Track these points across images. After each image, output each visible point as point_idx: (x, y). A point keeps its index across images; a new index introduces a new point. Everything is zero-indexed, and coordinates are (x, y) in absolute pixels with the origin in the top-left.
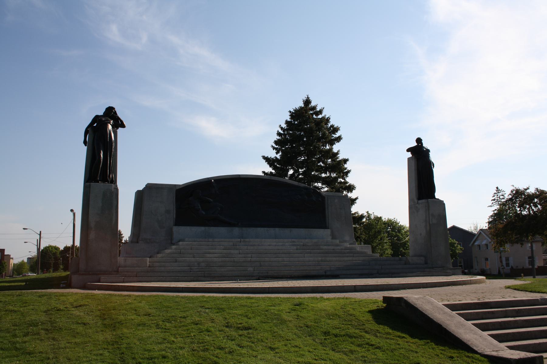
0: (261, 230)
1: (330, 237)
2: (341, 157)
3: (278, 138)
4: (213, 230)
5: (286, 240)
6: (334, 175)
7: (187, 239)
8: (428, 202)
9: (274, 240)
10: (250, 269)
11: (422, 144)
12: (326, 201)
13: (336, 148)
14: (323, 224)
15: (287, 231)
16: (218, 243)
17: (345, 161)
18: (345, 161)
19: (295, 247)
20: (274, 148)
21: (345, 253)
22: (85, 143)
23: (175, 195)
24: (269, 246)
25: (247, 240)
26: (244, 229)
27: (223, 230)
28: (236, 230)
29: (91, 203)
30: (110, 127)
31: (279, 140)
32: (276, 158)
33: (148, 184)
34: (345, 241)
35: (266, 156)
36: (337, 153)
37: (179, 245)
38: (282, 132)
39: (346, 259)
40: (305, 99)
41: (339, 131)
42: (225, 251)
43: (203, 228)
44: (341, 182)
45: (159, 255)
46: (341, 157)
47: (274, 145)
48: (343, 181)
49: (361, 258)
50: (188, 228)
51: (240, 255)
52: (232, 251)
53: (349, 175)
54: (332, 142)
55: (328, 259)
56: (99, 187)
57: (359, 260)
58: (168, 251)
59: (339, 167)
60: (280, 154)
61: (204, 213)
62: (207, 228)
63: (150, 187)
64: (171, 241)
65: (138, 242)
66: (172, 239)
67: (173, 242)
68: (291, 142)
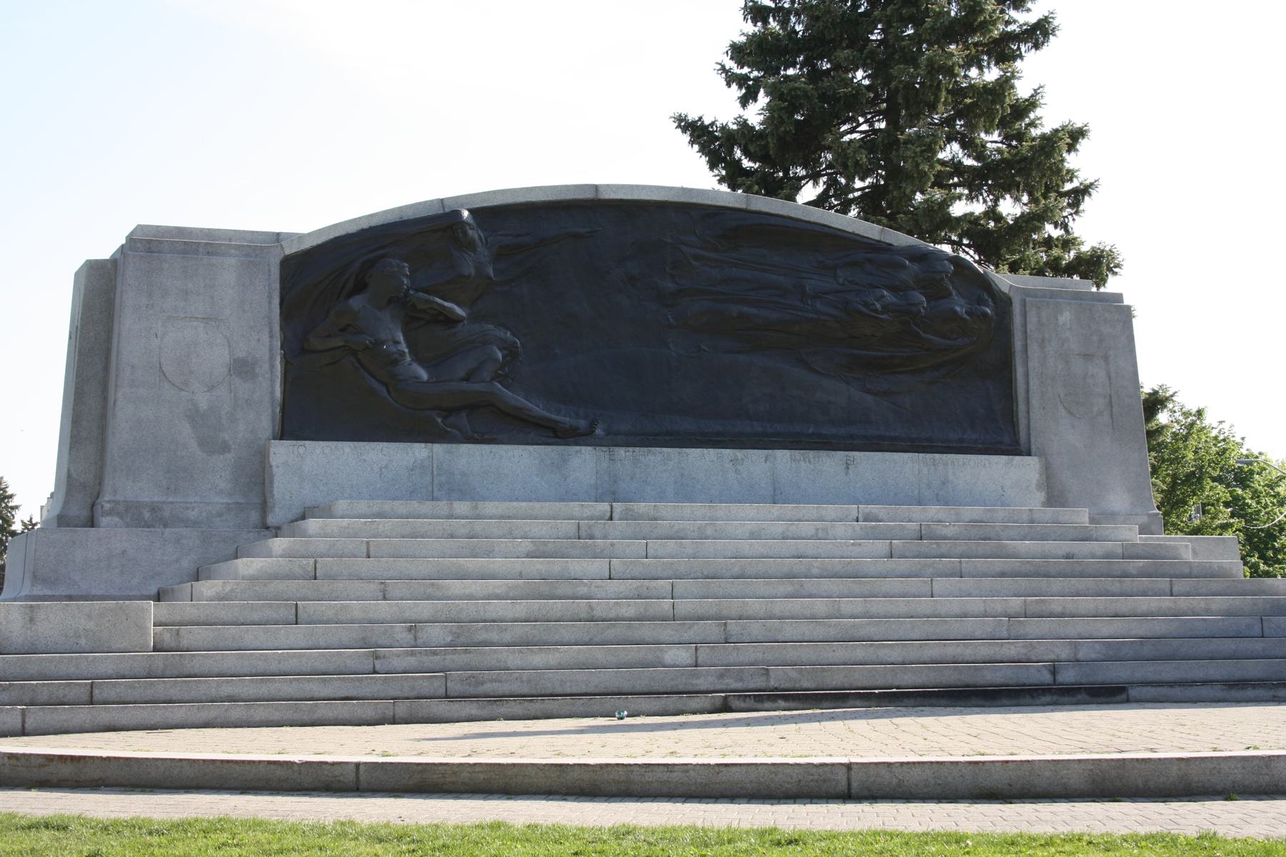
0: (703, 462)
1: (1040, 496)
2: (1048, 119)
3: (750, 28)
4: (470, 458)
5: (830, 510)
6: (1010, 208)
7: (342, 505)
9: (776, 509)
10: (681, 655)
12: (1017, 320)
13: (1031, 73)
14: (1000, 432)
15: (829, 464)
16: (497, 526)
17: (1076, 135)
18: (1076, 135)
19: (881, 546)
20: (731, 78)
21: (1125, 575)
23: (277, 285)
24: (753, 536)
25: (642, 507)
26: (621, 452)
27: (518, 459)
28: (584, 462)
31: (752, 39)
32: (744, 124)
33: (140, 228)
34: (1111, 516)
35: (693, 116)
36: (1032, 104)
37: (304, 534)
39: (1144, 603)
42: (539, 565)
43: (419, 451)
44: (1049, 243)
45: (207, 588)
46: (1048, 119)
47: (730, 64)
48: (1056, 233)
49: (1219, 602)
50: (346, 450)
51: (614, 586)
52: (575, 566)
53: (1087, 204)
54: (1004, 50)
55: (1057, 604)
57: (1208, 612)
58: (248, 566)
59: (1039, 165)
60: (763, 99)
61: (424, 375)
62: (438, 449)
63: (149, 247)
64: (259, 514)
65: (91, 523)
66: (264, 507)
67: (271, 520)
68: (813, 46)
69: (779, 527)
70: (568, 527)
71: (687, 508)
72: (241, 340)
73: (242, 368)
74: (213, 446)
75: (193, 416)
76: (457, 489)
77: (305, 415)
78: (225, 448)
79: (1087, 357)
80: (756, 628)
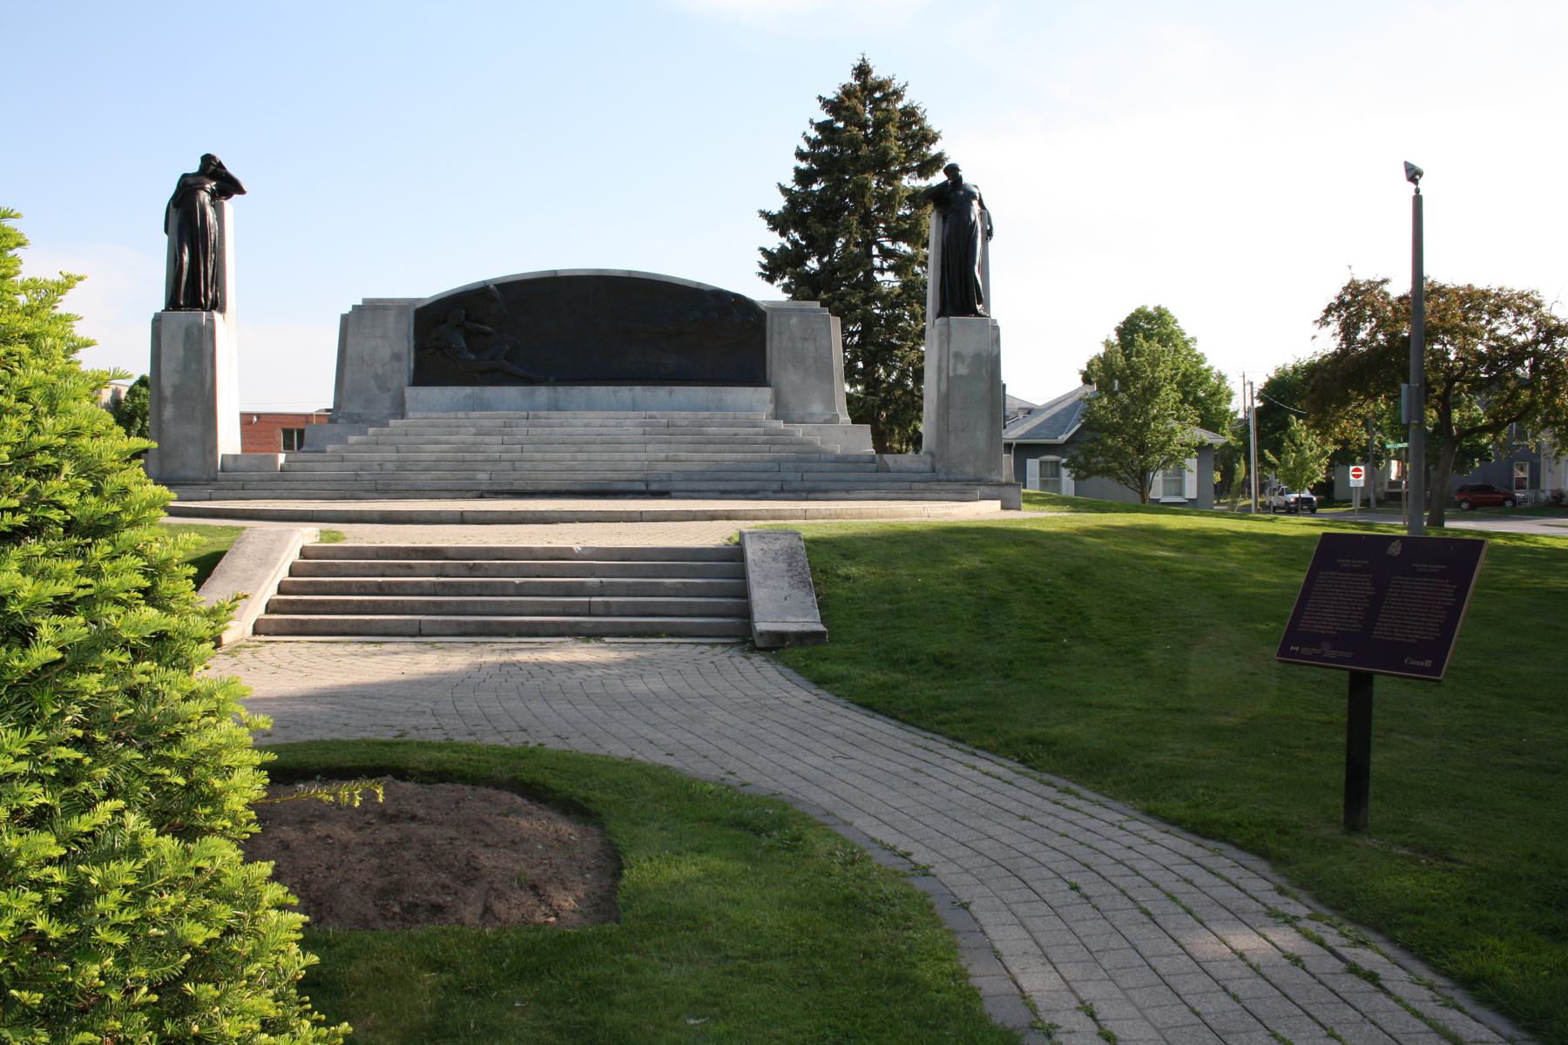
8: (948, 324)
11: (960, 179)
19: (640, 430)
22: (166, 231)
27: (511, 393)
28: (543, 393)
29: (164, 349)
30: (205, 197)
38: (806, 148)
40: (857, 64)
41: (939, 142)
43: (468, 390)
50: (437, 389)
56: (183, 316)
57: (762, 461)
62: (476, 389)
69: (599, 422)
70: (500, 422)
71: (592, 414)
72: (398, 343)
73: (397, 357)
74: (383, 388)
75: (377, 377)
76: (485, 406)
77: (423, 376)
78: (389, 390)
79: (805, 339)
80: (527, 465)
